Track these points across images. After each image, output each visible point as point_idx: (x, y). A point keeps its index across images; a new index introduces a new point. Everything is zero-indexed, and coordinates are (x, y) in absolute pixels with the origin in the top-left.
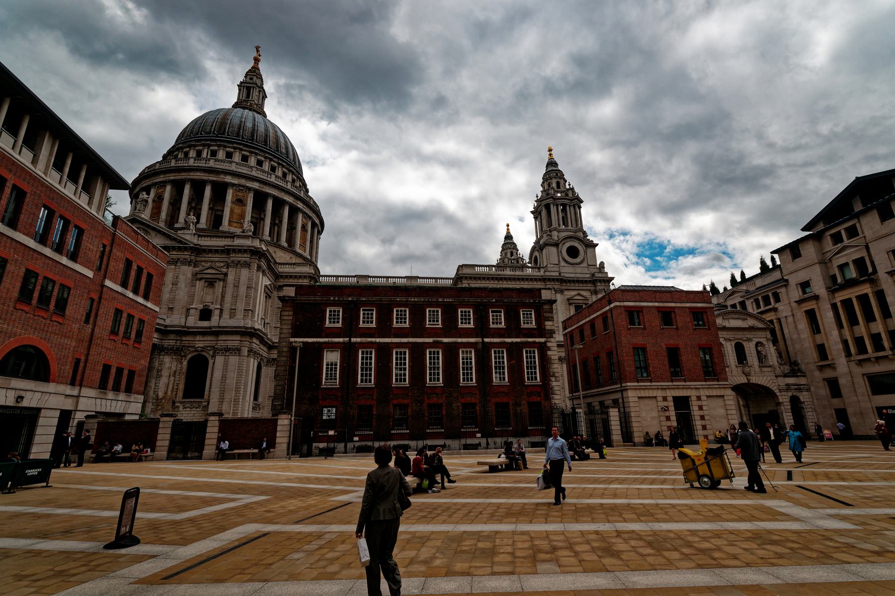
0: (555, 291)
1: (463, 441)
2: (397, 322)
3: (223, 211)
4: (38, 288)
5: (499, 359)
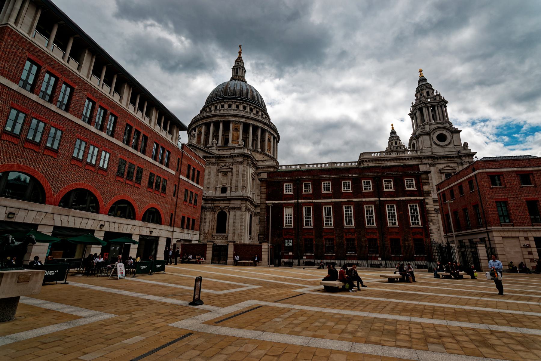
0: (429, 165)
1: (370, 262)
2: (324, 190)
3: (229, 136)
4: (155, 181)
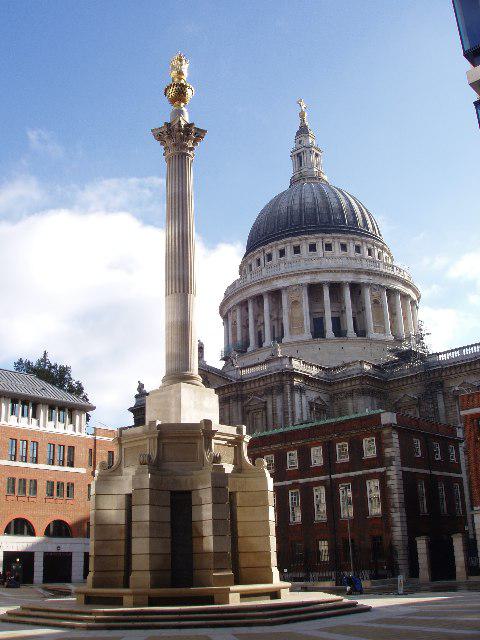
5: (346, 494)
